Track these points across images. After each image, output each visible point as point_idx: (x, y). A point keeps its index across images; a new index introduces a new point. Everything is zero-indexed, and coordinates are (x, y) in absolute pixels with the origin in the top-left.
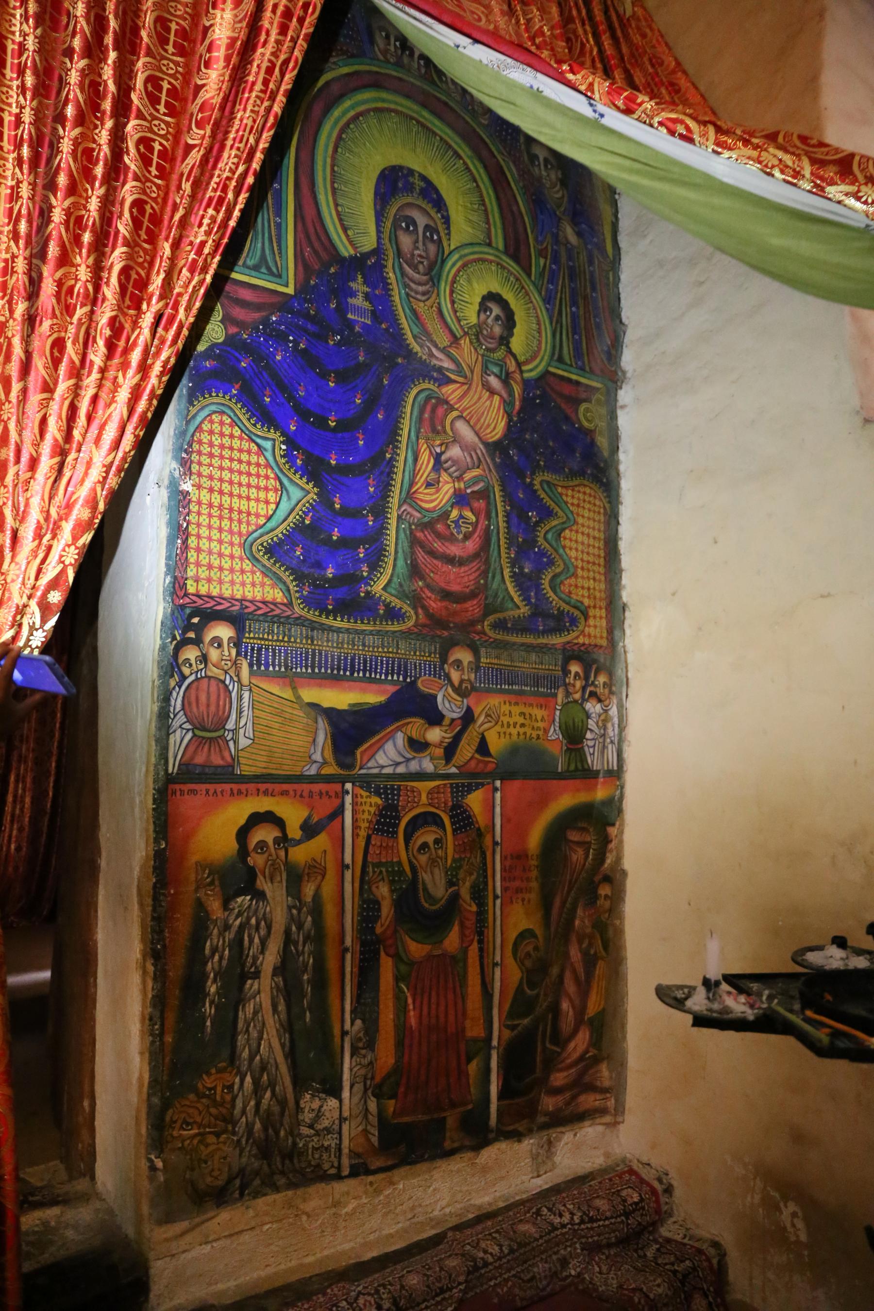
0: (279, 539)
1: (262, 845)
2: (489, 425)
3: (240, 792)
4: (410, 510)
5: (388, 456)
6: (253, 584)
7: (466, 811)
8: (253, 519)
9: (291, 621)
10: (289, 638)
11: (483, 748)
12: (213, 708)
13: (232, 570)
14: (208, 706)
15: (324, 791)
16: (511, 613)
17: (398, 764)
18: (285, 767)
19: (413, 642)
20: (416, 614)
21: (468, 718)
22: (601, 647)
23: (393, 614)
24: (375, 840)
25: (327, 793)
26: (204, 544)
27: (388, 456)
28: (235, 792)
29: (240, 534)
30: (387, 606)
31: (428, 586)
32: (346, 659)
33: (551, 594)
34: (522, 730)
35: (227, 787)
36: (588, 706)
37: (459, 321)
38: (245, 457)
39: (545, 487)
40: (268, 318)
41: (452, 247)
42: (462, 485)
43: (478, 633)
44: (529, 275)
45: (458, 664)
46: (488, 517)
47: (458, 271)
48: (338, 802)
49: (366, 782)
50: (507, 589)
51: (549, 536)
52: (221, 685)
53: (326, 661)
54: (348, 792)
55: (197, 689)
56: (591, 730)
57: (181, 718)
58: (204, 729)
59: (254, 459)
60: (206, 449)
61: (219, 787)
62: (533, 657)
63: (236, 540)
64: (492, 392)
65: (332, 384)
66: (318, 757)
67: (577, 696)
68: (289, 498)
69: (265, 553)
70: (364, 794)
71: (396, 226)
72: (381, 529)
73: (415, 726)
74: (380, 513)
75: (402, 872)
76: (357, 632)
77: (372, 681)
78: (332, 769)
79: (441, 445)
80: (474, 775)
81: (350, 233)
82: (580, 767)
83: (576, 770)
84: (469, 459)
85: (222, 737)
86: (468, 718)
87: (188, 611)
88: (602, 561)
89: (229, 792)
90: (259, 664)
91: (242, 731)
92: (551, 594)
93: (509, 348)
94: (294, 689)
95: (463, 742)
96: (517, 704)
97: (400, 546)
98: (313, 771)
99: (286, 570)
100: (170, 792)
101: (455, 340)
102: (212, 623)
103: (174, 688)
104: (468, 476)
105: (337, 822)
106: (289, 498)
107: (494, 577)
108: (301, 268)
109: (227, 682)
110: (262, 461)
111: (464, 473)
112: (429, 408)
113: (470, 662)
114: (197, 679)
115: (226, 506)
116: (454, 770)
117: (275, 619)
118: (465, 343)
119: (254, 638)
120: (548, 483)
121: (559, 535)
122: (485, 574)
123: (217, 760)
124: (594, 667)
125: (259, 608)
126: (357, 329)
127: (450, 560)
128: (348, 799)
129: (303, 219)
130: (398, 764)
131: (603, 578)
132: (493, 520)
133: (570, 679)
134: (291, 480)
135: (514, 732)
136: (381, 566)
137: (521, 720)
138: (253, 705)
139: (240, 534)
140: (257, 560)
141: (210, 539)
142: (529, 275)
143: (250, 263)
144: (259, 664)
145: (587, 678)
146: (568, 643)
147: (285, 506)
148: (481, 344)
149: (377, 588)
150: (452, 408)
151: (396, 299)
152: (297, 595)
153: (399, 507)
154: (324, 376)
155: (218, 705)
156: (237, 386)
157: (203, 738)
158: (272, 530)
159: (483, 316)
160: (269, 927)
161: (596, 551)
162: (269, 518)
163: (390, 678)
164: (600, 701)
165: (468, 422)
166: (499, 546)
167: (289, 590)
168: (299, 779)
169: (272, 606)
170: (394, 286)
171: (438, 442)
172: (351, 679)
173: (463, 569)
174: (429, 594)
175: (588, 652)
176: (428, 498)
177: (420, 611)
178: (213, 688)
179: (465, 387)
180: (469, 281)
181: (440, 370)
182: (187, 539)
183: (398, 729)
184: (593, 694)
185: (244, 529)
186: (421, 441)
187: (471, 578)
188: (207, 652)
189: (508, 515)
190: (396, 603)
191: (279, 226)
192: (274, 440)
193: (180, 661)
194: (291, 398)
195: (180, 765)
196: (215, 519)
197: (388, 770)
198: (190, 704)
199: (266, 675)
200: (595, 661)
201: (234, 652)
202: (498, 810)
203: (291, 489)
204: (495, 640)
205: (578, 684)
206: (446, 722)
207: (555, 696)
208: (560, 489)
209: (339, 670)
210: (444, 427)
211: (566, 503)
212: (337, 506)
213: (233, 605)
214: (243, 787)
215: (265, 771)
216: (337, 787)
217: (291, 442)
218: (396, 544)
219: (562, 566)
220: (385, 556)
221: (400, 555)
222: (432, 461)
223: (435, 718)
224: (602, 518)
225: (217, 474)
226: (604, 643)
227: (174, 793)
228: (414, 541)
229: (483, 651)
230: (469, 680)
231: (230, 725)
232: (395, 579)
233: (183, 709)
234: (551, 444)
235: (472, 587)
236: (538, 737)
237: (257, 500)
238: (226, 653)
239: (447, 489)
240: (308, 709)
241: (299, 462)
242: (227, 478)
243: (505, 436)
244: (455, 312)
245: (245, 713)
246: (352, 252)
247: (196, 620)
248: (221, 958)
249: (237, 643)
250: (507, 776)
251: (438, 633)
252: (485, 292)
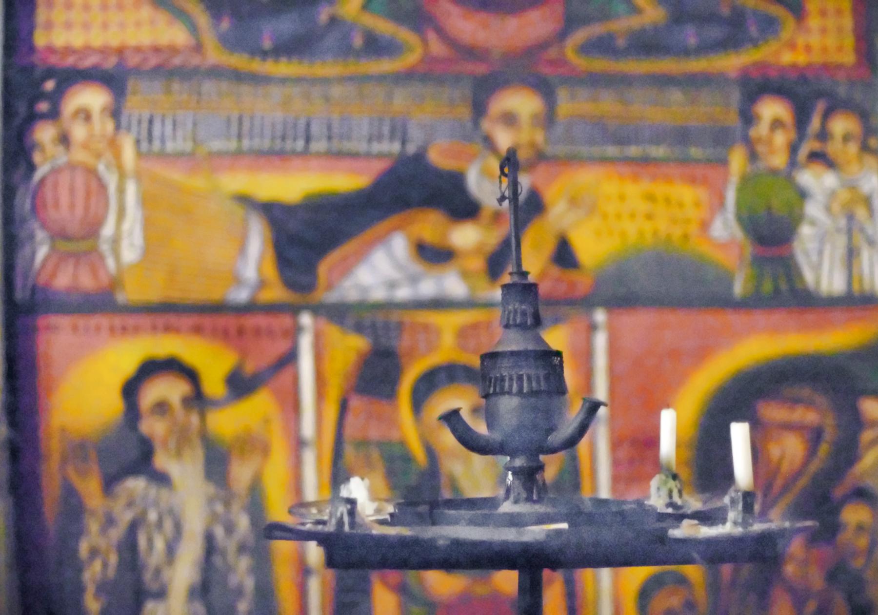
1: (162, 407)
3: (124, 329)
14: (72, 206)
24: (356, 403)
36: (807, 178)
45: (510, 119)
56: (813, 223)
75: (407, 458)
76: (315, 81)
77: (340, 155)
78: (276, 293)
82: (784, 286)
83: (777, 291)
105: (285, 377)
123: (87, 282)
133: (761, 129)
160: (178, 528)
168: (218, 308)
172: (305, 153)
178: (80, 181)
199: (163, 156)
206: (486, 214)
209: (283, 138)
216: (285, 321)
231: (108, 230)
248: (105, 565)
249: (115, 113)
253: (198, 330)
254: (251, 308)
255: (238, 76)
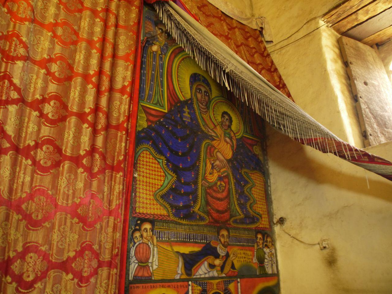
0: (165, 193)
2: (227, 154)
3: (154, 287)
4: (205, 182)
5: (197, 164)
6: (157, 209)
7: (229, 291)
8: (156, 186)
9: (169, 221)
10: (169, 228)
11: (233, 267)
12: (145, 255)
13: (150, 204)
14: (143, 254)
15: (182, 285)
16: (238, 217)
17: (206, 273)
18: (169, 276)
19: (208, 228)
20: (209, 218)
21: (227, 256)
22: (267, 228)
23: (202, 219)
25: (183, 286)
26: (141, 195)
27: (197, 164)
28: (152, 286)
29: (152, 191)
30: (200, 216)
31: (212, 209)
32: (187, 235)
33: (250, 210)
34: (245, 259)
35: (149, 285)
36: (265, 250)
37: (216, 120)
38: (154, 165)
39: (245, 173)
40: (160, 120)
41: (213, 98)
42: (220, 174)
43: (229, 225)
44: (235, 106)
45: (223, 235)
46: (229, 184)
47: (215, 105)
48: (186, 289)
49: (196, 281)
50: (236, 209)
51: (248, 190)
52: (147, 246)
53: (181, 236)
54: (190, 285)
55: (139, 247)
57: (134, 258)
58: (142, 263)
59: (156, 166)
60: (142, 163)
61: (147, 285)
62: (246, 232)
63: (151, 193)
64: (227, 143)
65: (180, 141)
66: (179, 272)
67: (261, 246)
68: (168, 179)
69: (161, 198)
70: (196, 285)
71: (196, 91)
72: (196, 190)
73: (211, 259)
74: (196, 183)
77: (196, 243)
78: (184, 277)
79: (213, 160)
80: (230, 277)
81: (183, 93)
82: (264, 273)
84: (222, 165)
85: (148, 265)
86: (227, 256)
87: (136, 219)
88: (264, 198)
89: (150, 287)
90: (159, 238)
91: (154, 263)
92: (250, 210)
93: (231, 129)
94: (171, 246)
95: (227, 264)
96: (242, 250)
97: (202, 195)
98: (178, 278)
99: (167, 204)
100: (130, 287)
101: (215, 126)
102: (144, 223)
103: (132, 247)
104: (222, 171)
106: (168, 179)
107: (232, 205)
108: (169, 104)
109: (149, 244)
110: (159, 167)
111: (221, 169)
112: (209, 148)
113: (227, 235)
114: (140, 244)
115: (148, 182)
116: (224, 275)
117: (164, 221)
118: (218, 127)
119: (158, 228)
120: (246, 172)
121: (251, 190)
122: (229, 203)
123: (146, 274)
124: (266, 235)
125: (159, 217)
126: (186, 123)
127: (219, 199)
128: (190, 288)
129: (169, 89)
130: (206, 273)
131: (265, 204)
132: (230, 186)
133: (258, 240)
134: (168, 173)
135: (242, 260)
136: (197, 202)
137: (244, 256)
138: (159, 253)
139: (152, 191)
140: (158, 200)
141: (143, 193)
142: (235, 106)
143: (154, 102)
144: (159, 238)
145: (264, 239)
146: (257, 227)
147: (166, 182)
148: (223, 128)
149: (196, 209)
150: (215, 148)
151: (197, 114)
152: (171, 212)
153: (202, 181)
154: (177, 138)
155: (146, 253)
156: (151, 142)
157: (141, 266)
158: (162, 190)
159: (223, 119)
161: (262, 195)
162: (161, 186)
163: (202, 241)
164: (268, 248)
165: (220, 153)
166: (233, 194)
167: (168, 211)
169: (164, 217)
170: (196, 110)
171: (212, 160)
172: (189, 242)
173: (223, 202)
174: (212, 211)
175: (264, 230)
176: (210, 178)
177: (210, 217)
178: (145, 247)
179: (219, 141)
180: (218, 108)
181: (211, 136)
182: (136, 193)
183: (205, 260)
184: (266, 246)
185: (154, 190)
186: (207, 159)
187: (225, 205)
188: (143, 234)
189: (235, 184)
190: (202, 214)
191: (162, 91)
192: (162, 159)
193: (134, 237)
194: (168, 146)
195: (134, 276)
196: (145, 186)
197: (203, 276)
198: (137, 253)
200: (266, 233)
201: (151, 233)
202: (239, 290)
203: (168, 176)
204: (234, 227)
205: (261, 242)
206: (221, 257)
207: (254, 246)
208: (250, 174)
209: (185, 239)
210: (214, 155)
211: (252, 179)
212: (183, 181)
213: (151, 216)
214: (155, 284)
215: (162, 278)
216: (186, 283)
217: (168, 160)
218: (201, 194)
219: (253, 200)
220: (198, 198)
221: (203, 198)
222: (211, 166)
223: (217, 256)
224: (263, 183)
225: (145, 171)
226: (268, 227)
227: (131, 288)
228: (207, 193)
229: (230, 231)
230: (227, 241)
231: (150, 261)
232: (202, 207)
233: (135, 255)
234: (246, 159)
235: (226, 208)
236: (250, 262)
237: (158, 180)
238: (149, 234)
239: (216, 175)
240: (176, 254)
241: (170, 167)
242: (148, 172)
243: (232, 157)
244: (215, 117)
245: (155, 256)
246: (184, 99)
247: (139, 222)
249: (152, 230)
250: (242, 277)
251: (216, 225)
252: (223, 112)
253: (169, 287)
254: (178, 281)
255: (177, 223)
